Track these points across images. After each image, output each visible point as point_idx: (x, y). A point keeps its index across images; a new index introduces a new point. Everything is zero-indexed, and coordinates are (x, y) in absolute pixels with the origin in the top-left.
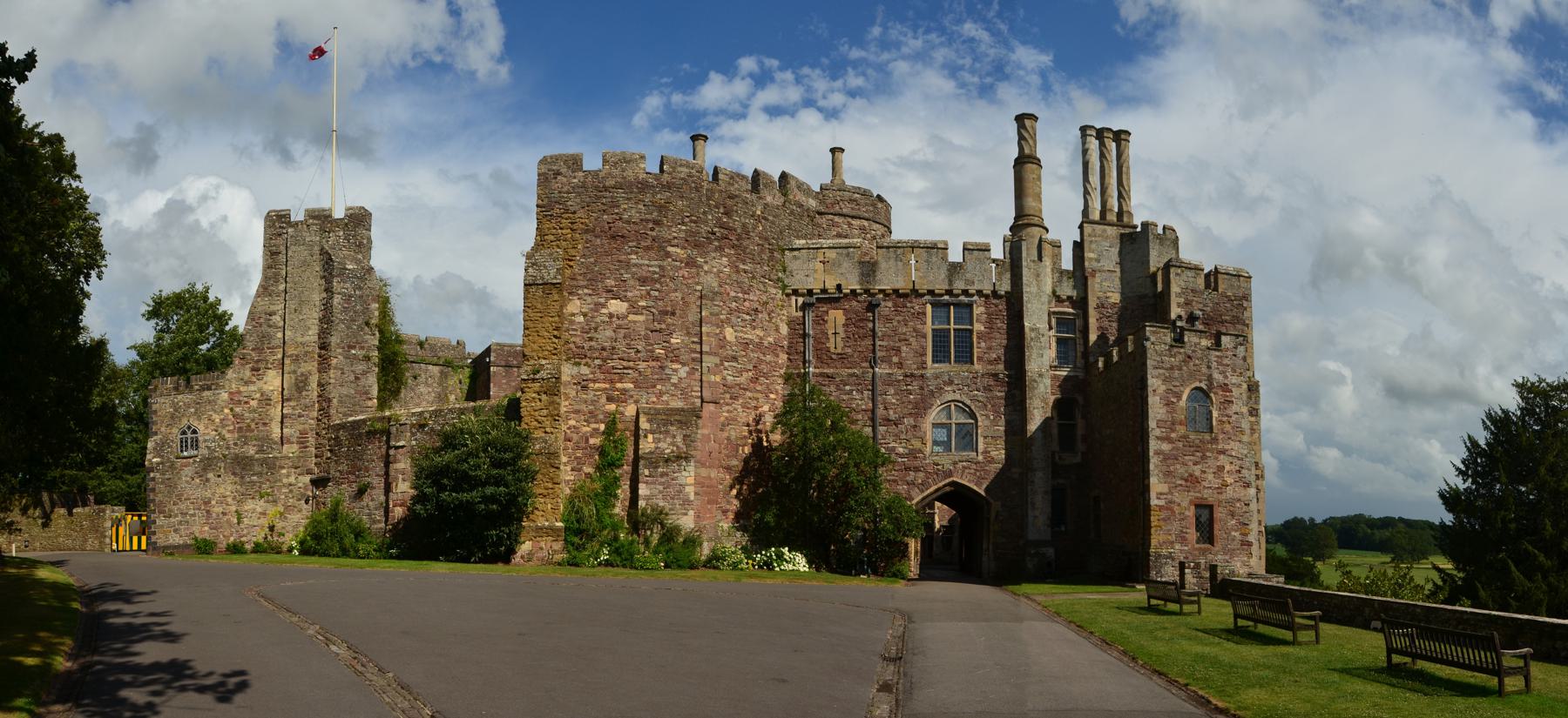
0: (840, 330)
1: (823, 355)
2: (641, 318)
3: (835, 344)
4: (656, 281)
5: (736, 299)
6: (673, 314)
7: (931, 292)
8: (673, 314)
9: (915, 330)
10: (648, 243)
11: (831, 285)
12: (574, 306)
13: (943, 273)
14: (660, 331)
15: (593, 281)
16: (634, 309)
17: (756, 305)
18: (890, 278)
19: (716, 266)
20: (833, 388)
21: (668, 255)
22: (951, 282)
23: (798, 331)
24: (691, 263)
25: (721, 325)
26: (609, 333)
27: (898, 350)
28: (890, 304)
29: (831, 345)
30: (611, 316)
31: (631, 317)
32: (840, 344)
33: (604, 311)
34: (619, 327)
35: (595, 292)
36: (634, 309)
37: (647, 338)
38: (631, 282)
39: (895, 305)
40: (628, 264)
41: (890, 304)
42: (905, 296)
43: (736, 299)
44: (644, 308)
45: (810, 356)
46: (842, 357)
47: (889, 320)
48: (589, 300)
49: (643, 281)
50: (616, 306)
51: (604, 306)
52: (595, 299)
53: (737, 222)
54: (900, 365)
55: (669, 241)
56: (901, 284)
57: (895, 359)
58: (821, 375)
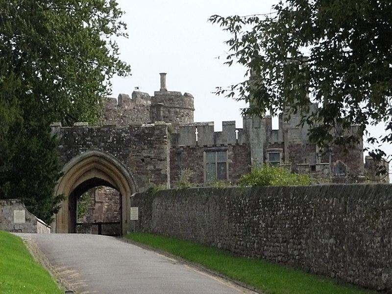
7: (206, 146)
13: (211, 137)
22: (215, 141)
28: (185, 153)
39: (188, 153)
41: (185, 153)
42: (193, 149)
56: (191, 143)
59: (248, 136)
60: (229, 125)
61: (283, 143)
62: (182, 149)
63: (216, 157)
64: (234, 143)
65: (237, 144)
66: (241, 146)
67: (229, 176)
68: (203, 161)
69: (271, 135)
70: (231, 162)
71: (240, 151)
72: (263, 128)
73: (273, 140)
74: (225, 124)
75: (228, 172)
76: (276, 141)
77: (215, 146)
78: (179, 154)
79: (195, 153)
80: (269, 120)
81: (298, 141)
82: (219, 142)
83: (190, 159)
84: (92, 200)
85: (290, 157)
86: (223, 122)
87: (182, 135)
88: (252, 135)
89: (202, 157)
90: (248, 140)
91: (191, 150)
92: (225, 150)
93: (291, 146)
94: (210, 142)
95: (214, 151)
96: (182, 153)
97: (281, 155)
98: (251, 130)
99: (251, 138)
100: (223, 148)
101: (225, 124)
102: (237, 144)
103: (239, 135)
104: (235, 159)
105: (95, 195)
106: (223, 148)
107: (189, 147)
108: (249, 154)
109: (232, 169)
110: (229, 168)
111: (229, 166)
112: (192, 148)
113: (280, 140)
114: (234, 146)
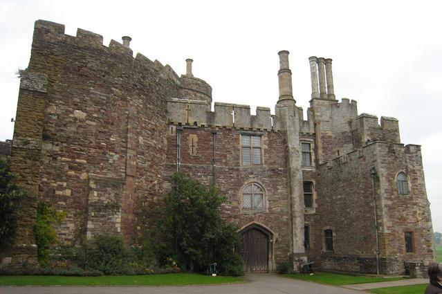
0: (195, 144)
1: (186, 157)
2: (94, 124)
3: (193, 152)
4: (103, 104)
5: (145, 122)
6: (112, 124)
7: (242, 129)
8: (112, 124)
9: (234, 147)
10: (102, 83)
11: (191, 121)
12: (52, 109)
13: (248, 120)
14: (105, 132)
15: (66, 97)
16: (90, 117)
17: (154, 127)
18: (220, 122)
19: (136, 103)
21: (112, 92)
23: (172, 143)
24: (123, 99)
25: (138, 134)
26: (73, 129)
27: (225, 157)
28: (221, 133)
29: (190, 152)
30: (75, 119)
31: (87, 122)
32: (195, 152)
33: (72, 115)
34: (80, 126)
35: (66, 104)
36: (90, 117)
37: (96, 135)
38: (90, 102)
39: (224, 134)
40: (88, 92)
41: (221, 133)
42: (230, 130)
43: (145, 122)
44: (96, 118)
45: (179, 156)
46: (196, 158)
47: (220, 141)
48: (62, 107)
49: (97, 103)
50: (79, 114)
51: (72, 113)
52: (67, 108)
53: (147, 82)
54: (226, 164)
55: (113, 84)
56: (227, 124)
57: (224, 161)
58: (185, 166)
59: (283, 124)
60: (263, 111)
61: (314, 134)
63: (255, 141)
64: (269, 129)
65: (273, 130)
66: (275, 133)
67: (265, 162)
68: (239, 144)
69: (303, 126)
71: (275, 138)
72: (297, 117)
73: (305, 130)
74: (259, 109)
76: (308, 132)
77: (251, 129)
78: (214, 134)
80: (301, 111)
81: (330, 133)
82: (256, 126)
83: (226, 141)
84: (123, 172)
85: (323, 148)
86: (258, 107)
87: (218, 114)
88: (288, 123)
89: (238, 139)
90: (284, 127)
91: (227, 130)
92: (260, 136)
93: (323, 137)
94: (247, 126)
95: (250, 135)
96: (218, 133)
97: (312, 146)
98: (287, 117)
99: (288, 125)
100: (259, 133)
101: (259, 109)
102: (273, 130)
103: (275, 122)
104: (270, 145)
105: (126, 167)
106: (259, 133)
108: (285, 142)
109: (267, 155)
112: (228, 129)
113: (312, 131)
114: (269, 132)
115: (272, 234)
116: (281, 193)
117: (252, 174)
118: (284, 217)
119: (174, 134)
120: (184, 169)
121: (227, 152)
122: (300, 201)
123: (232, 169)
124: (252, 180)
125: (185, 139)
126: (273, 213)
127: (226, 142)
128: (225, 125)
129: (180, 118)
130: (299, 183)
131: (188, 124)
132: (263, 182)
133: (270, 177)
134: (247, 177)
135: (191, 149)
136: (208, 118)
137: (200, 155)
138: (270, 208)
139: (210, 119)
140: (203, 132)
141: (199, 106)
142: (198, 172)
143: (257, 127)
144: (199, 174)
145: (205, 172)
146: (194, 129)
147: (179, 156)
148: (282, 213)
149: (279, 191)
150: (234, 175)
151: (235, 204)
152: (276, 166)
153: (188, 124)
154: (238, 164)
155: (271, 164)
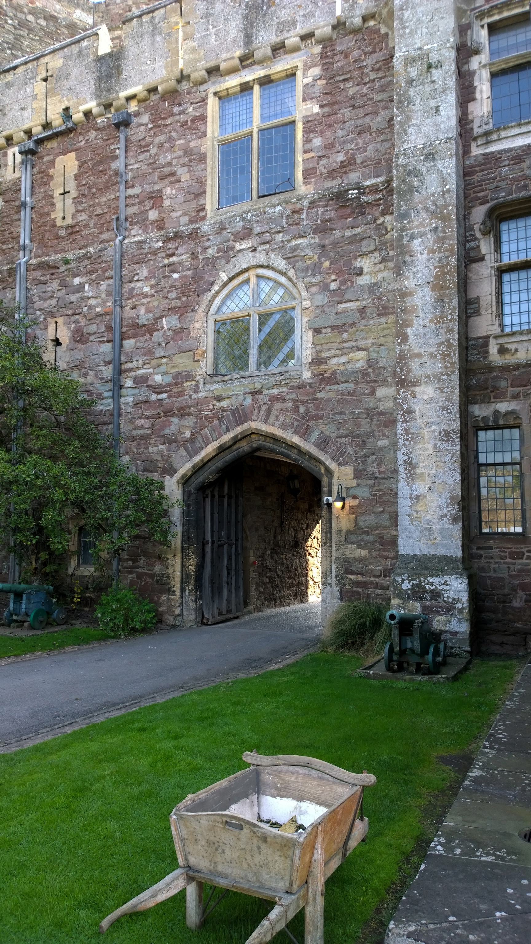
0: (71, 186)
9: (187, 152)
20: (54, 285)
22: (248, 38)
27: (156, 198)
28: (145, 119)
29: (57, 215)
32: (71, 209)
42: (172, 95)
45: (25, 239)
46: (73, 230)
47: (144, 148)
57: (153, 215)
62: (133, 107)
66: (356, 31)
70: (316, 109)
71: (356, 53)
75: (299, 158)
78: (124, 123)
79: (176, 109)
87: (132, 52)
89: (203, 118)
96: (135, 121)
107: (153, 90)
109: (317, 142)
110: (307, 141)
111: (307, 131)
115: (329, 472)
116: (372, 288)
117: (247, 233)
118: (381, 392)
119: (17, 175)
120: (37, 274)
121: (162, 178)
122: (440, 299)
123: (177, 236)
124: (244, 261)
125: (42, 180)
126: (331, 379)
127: (161, 146)
128: (150, 81)
129: (26, 114)
130: (439, 214)
131: (46, 126)
132: (292, 257)
133: (323, 228)
134: (228, 253)
135: (59, 205)
136: (99, 79)
137: (83, 217)
138: (317, 361)
139: (109, 76)
140: (92, 134)
141: (75, 49)
142: (74, 276)
143: (274, 39)
144: (77, 281)
145: (94, 267)
146: (63, 133)
147: (25, 239)
148: (371, 376)
149: (364, 280)
150: (182, 256)
151: (183, 362)
152: (354, 177)
153: (46, 126)
154: (199, 214)
155: (332, 174)
